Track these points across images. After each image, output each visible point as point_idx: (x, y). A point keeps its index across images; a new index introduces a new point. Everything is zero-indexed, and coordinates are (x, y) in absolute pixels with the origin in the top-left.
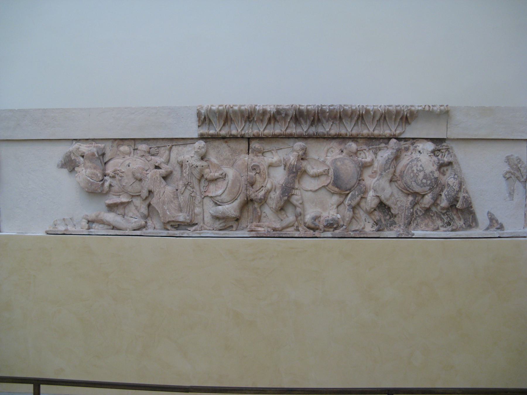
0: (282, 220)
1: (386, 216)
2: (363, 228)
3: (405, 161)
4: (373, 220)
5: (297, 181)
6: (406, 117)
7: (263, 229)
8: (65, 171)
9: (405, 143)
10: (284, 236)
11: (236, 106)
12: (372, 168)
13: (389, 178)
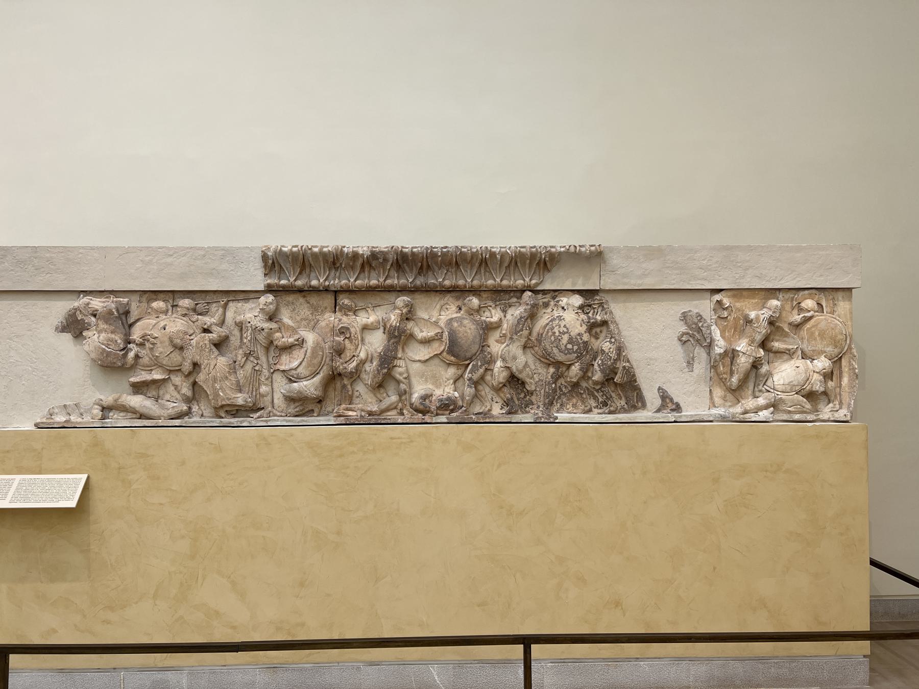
1: (519, 394)
2: (490, 410)
3: (543, 320)
5: (400, 348)
6: (544, 262)
7: (355, 414)
8: (67, 336)
11: (316, 247)
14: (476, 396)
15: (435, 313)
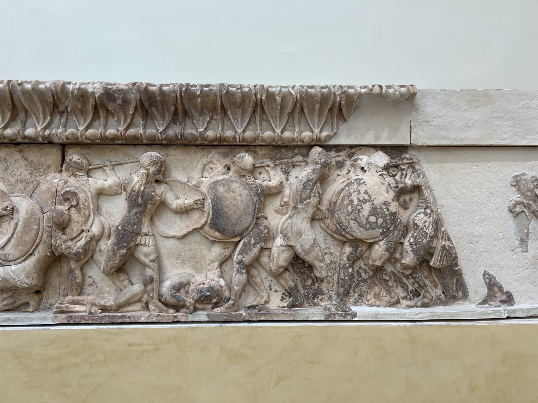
0: (121, 290)
2: (267, 302)
3: (337, 183)
4: (283, 287)
7: (83, 308)
9: (337, 154)
10: (119, 321)
12: (279, 198)
13: (310, 215)
14: (249, 283)
15: (195, 175)
